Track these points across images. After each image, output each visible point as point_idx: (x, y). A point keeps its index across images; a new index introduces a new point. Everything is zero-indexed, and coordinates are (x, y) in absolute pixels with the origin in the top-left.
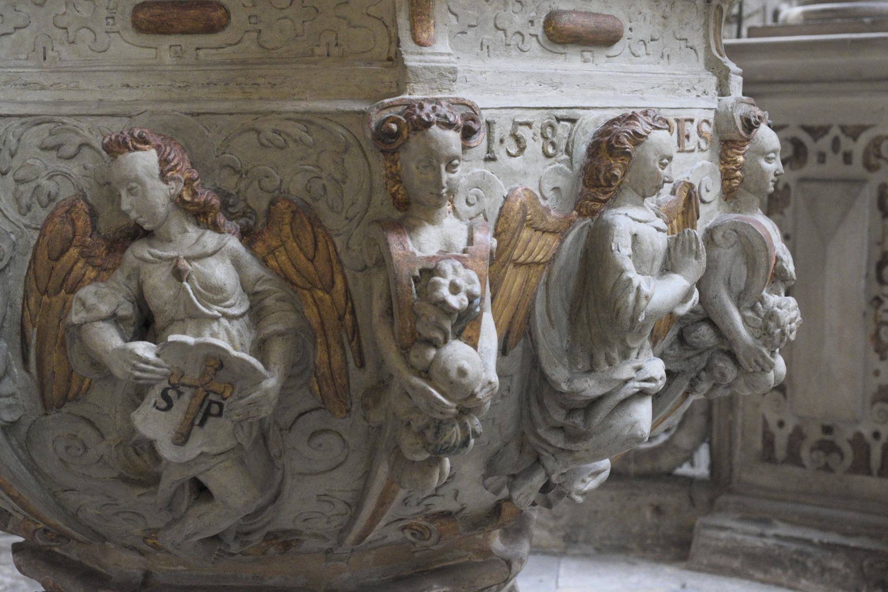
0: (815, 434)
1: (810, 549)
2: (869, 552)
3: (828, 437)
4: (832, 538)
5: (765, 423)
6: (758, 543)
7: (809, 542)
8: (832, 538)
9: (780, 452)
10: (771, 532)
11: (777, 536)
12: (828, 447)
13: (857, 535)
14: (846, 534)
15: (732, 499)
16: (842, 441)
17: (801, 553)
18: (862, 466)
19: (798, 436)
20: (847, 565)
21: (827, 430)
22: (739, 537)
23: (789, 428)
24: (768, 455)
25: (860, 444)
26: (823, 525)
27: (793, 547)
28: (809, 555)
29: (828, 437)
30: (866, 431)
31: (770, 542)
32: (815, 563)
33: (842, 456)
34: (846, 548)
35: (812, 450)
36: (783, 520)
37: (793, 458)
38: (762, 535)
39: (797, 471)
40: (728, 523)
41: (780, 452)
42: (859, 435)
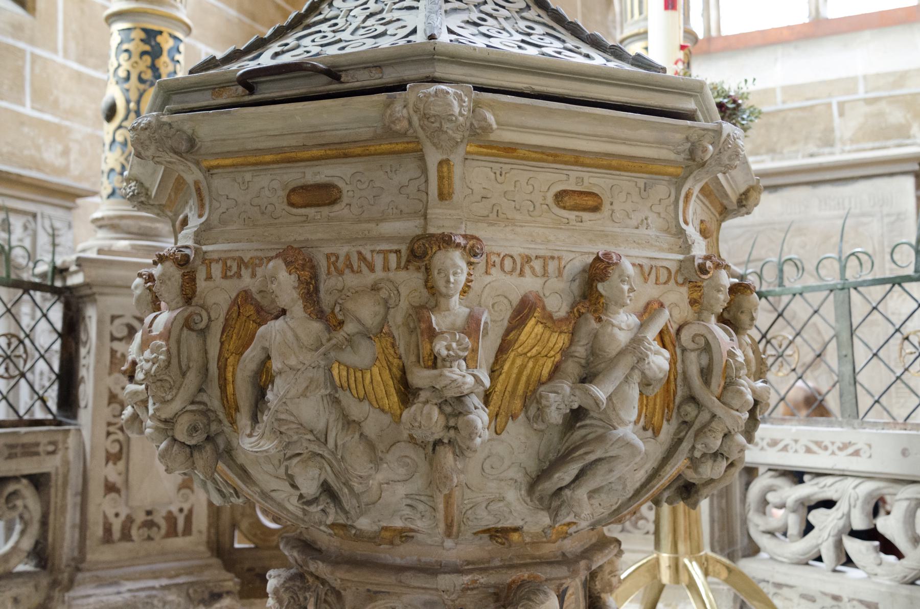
0: (141, 517)
1: (154, 592)
2: (192, 584)
3: (149, 518)
4: (164, 582)
5: (105, 517)
6: (118, 598)
7: (153, 588)
8: (164, 582)
9: (116, 534)
10: (123, 589)
11: (130, 591)
12: (150, 525)
13: (177, 576)
14: (170, 577)
15: (88, 574)
16: (159, 518)
17: (149, 597)
18: (172, 532)
19: (130, 520)
20: (179, 596)
21: (149, 513)
22: (104, 598)
23: (123, 517)
24: (108, 537)
25: (171, 519)
26: (155, 575)
27: (143, 594)
28: (155, 596)
29: (149, 518)
30: (174, 509)
31: (127, 595)
32: (159, 601)
33: (159, 527)
34: (176, 585)
35: (139, 528)
36: (127, 579)
37: (126, 536)
38: (119, 593)
39: (128, 545)
40: (91, 592)
41: (116, 534)
42: (170, 513)
